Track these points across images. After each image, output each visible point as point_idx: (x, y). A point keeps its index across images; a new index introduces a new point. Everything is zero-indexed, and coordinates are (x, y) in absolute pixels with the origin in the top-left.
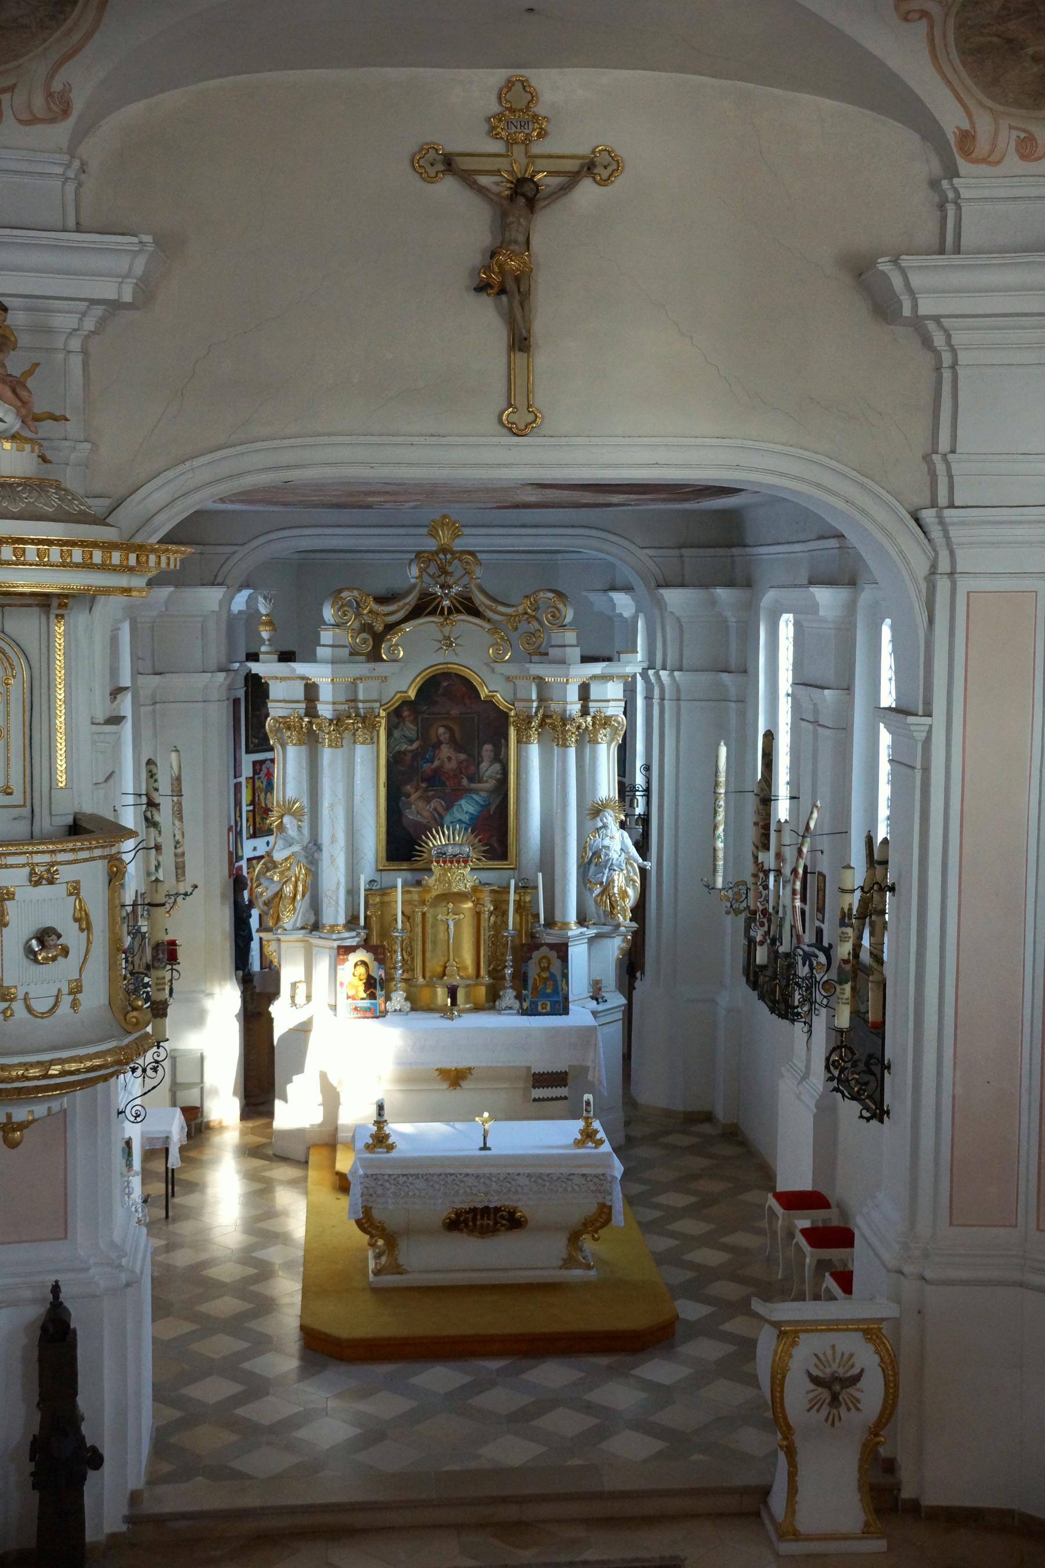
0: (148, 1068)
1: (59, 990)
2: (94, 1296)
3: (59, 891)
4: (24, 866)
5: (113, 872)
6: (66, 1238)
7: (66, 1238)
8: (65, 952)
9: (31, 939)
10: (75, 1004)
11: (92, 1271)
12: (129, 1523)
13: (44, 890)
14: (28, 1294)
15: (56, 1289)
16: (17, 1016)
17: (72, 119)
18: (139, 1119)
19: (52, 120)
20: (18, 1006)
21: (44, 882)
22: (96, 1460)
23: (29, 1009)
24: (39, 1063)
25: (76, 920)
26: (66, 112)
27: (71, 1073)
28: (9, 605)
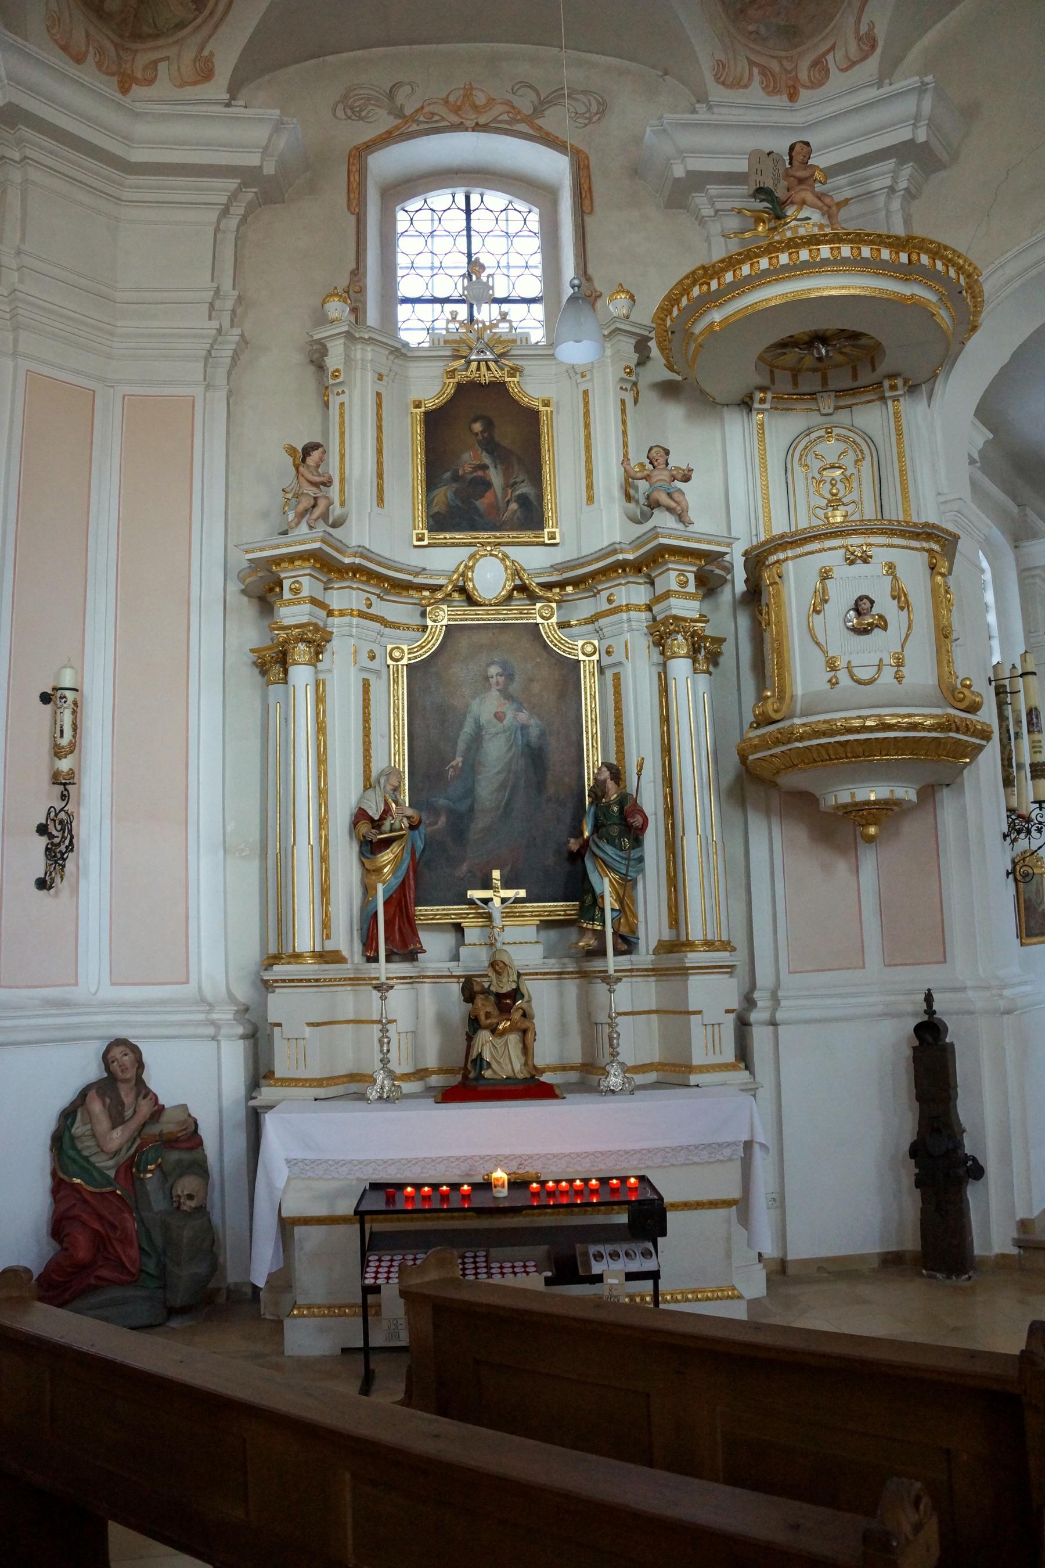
0: (1032, 830)
1: (881, 660)
2: (971, 1013)
3: (876, 568)
4: (840, 547)
5: (932, 564)
6: (945, 961)
7: (945, 961)
8: (882, 624)
9: (848, 612)
10: (899, 678)
11: (970, 993)
12: (1019, 1247)
13: (859, 567)
14: (909, 1008)
15: (929, 998)
16: (842, 683)
17: (879, 50)
18: (1027, 879)
19: (864, 58)
20: (843, 676)
21: (859, 561)
22: (977, 1172)
23: (852, 676)
24: (859, 717)
25: (894, 598)
26: (873, 47)
27: (889, 727)
28: (857, 404)
